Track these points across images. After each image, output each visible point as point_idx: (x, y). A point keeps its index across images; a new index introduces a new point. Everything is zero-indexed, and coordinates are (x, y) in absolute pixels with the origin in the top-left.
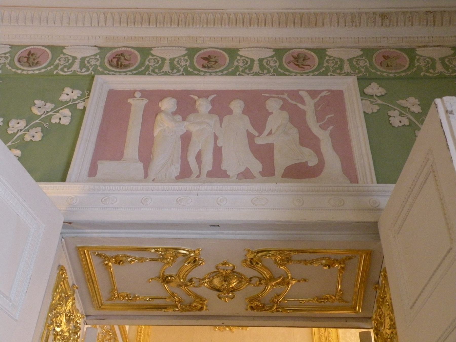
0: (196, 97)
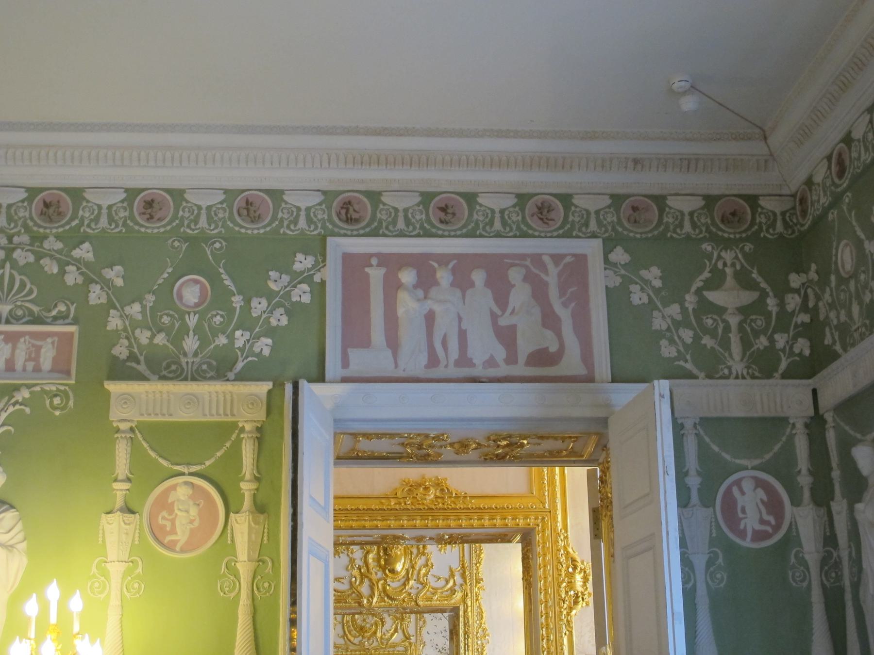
0: (436, 265)
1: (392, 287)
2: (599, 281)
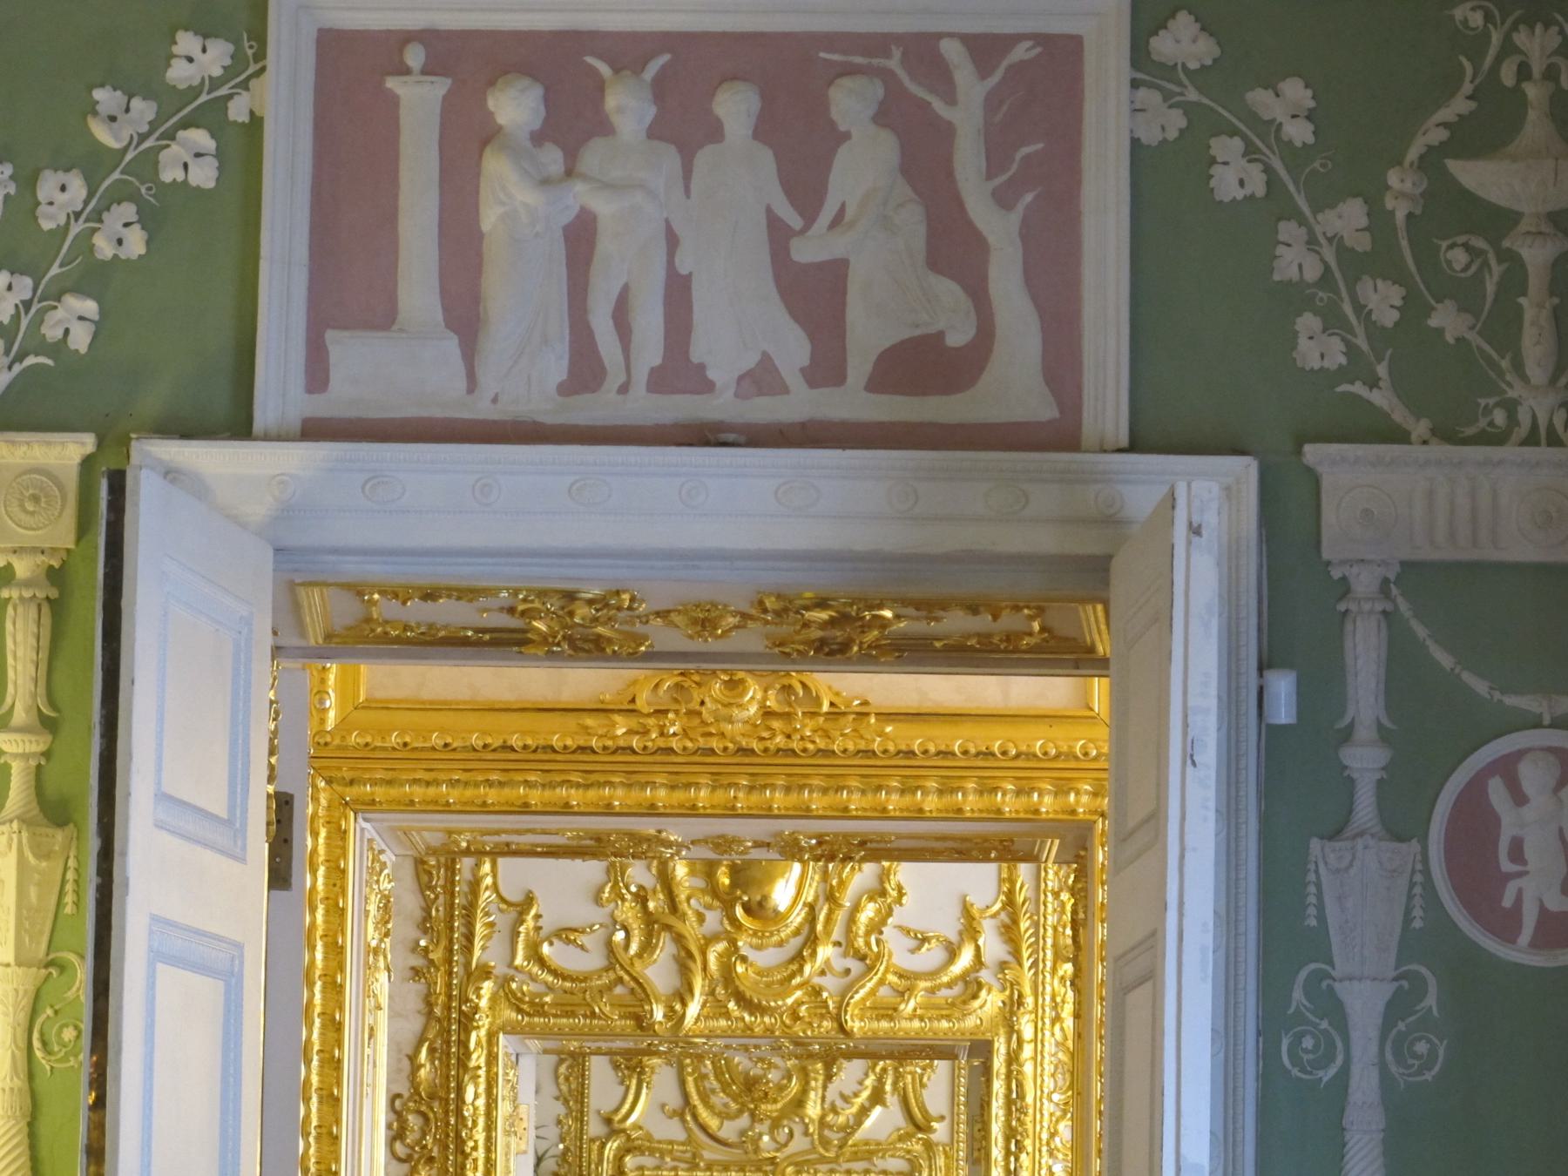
0: (604, 69)
1: (466, 138)
2: (1111, 122)
